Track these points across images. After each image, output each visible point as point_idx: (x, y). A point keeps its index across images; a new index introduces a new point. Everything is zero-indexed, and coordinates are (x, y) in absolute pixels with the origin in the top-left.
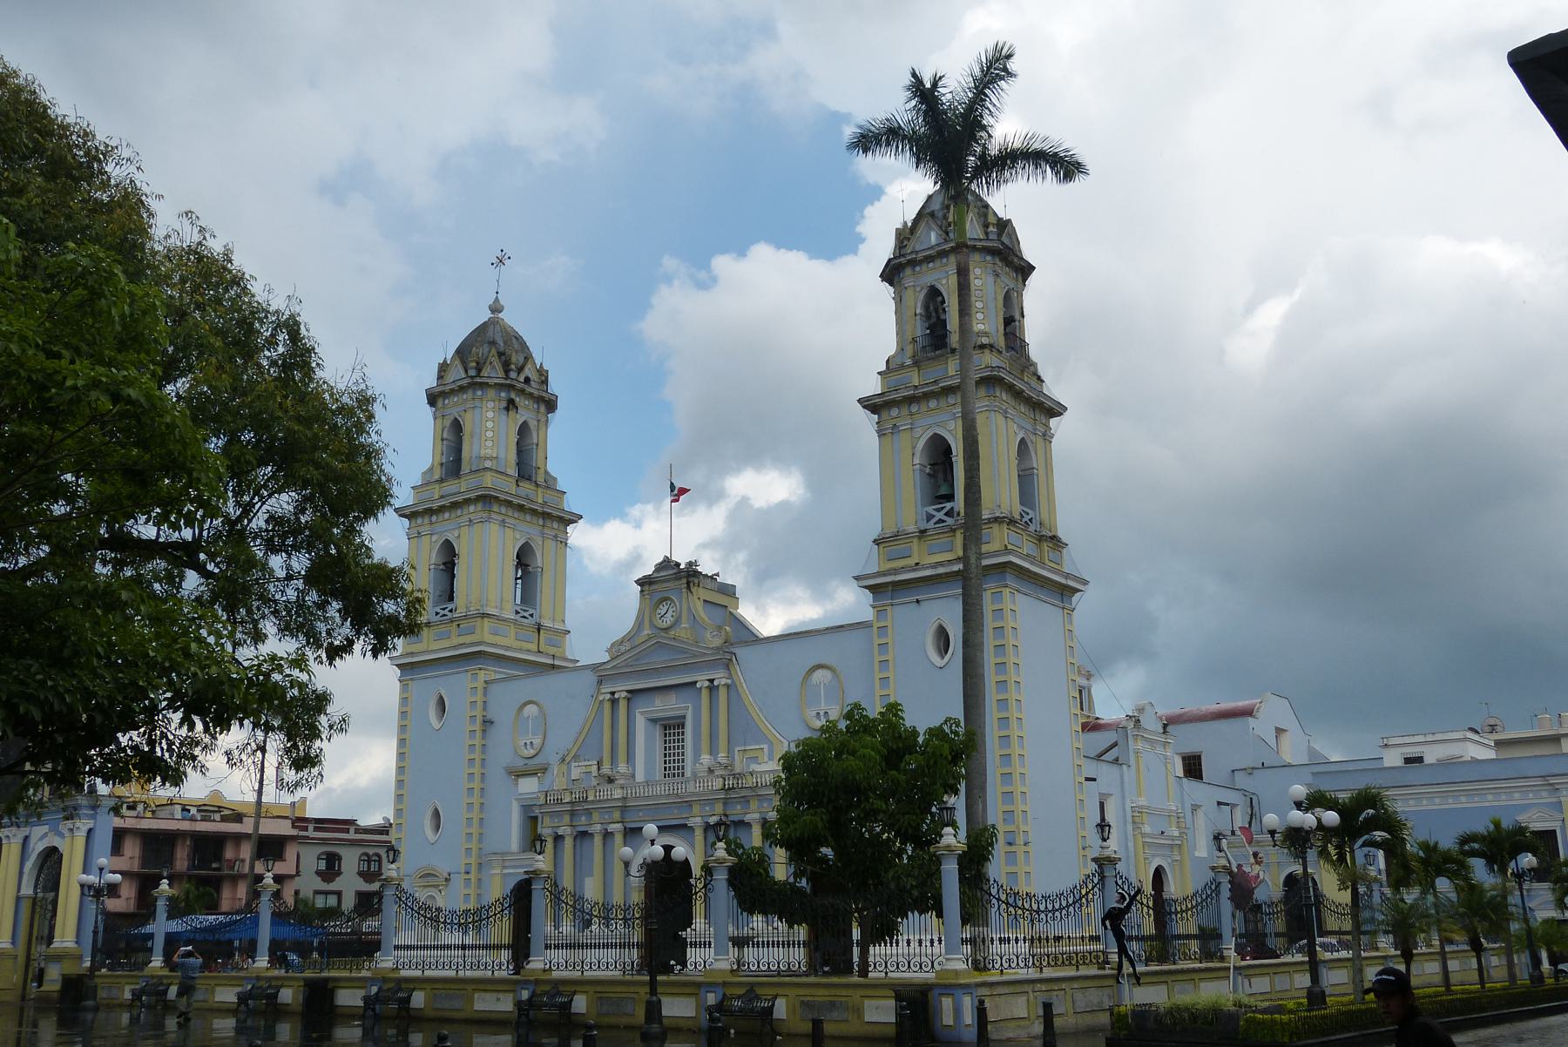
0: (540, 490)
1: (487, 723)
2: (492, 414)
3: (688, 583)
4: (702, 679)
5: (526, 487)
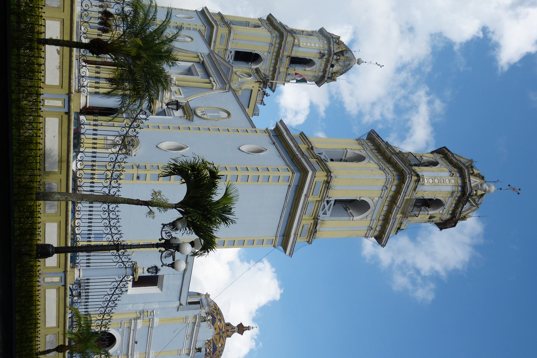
0: (285, 70)
2: (318, 46)
3: (260, 82)
5: (286, 61)
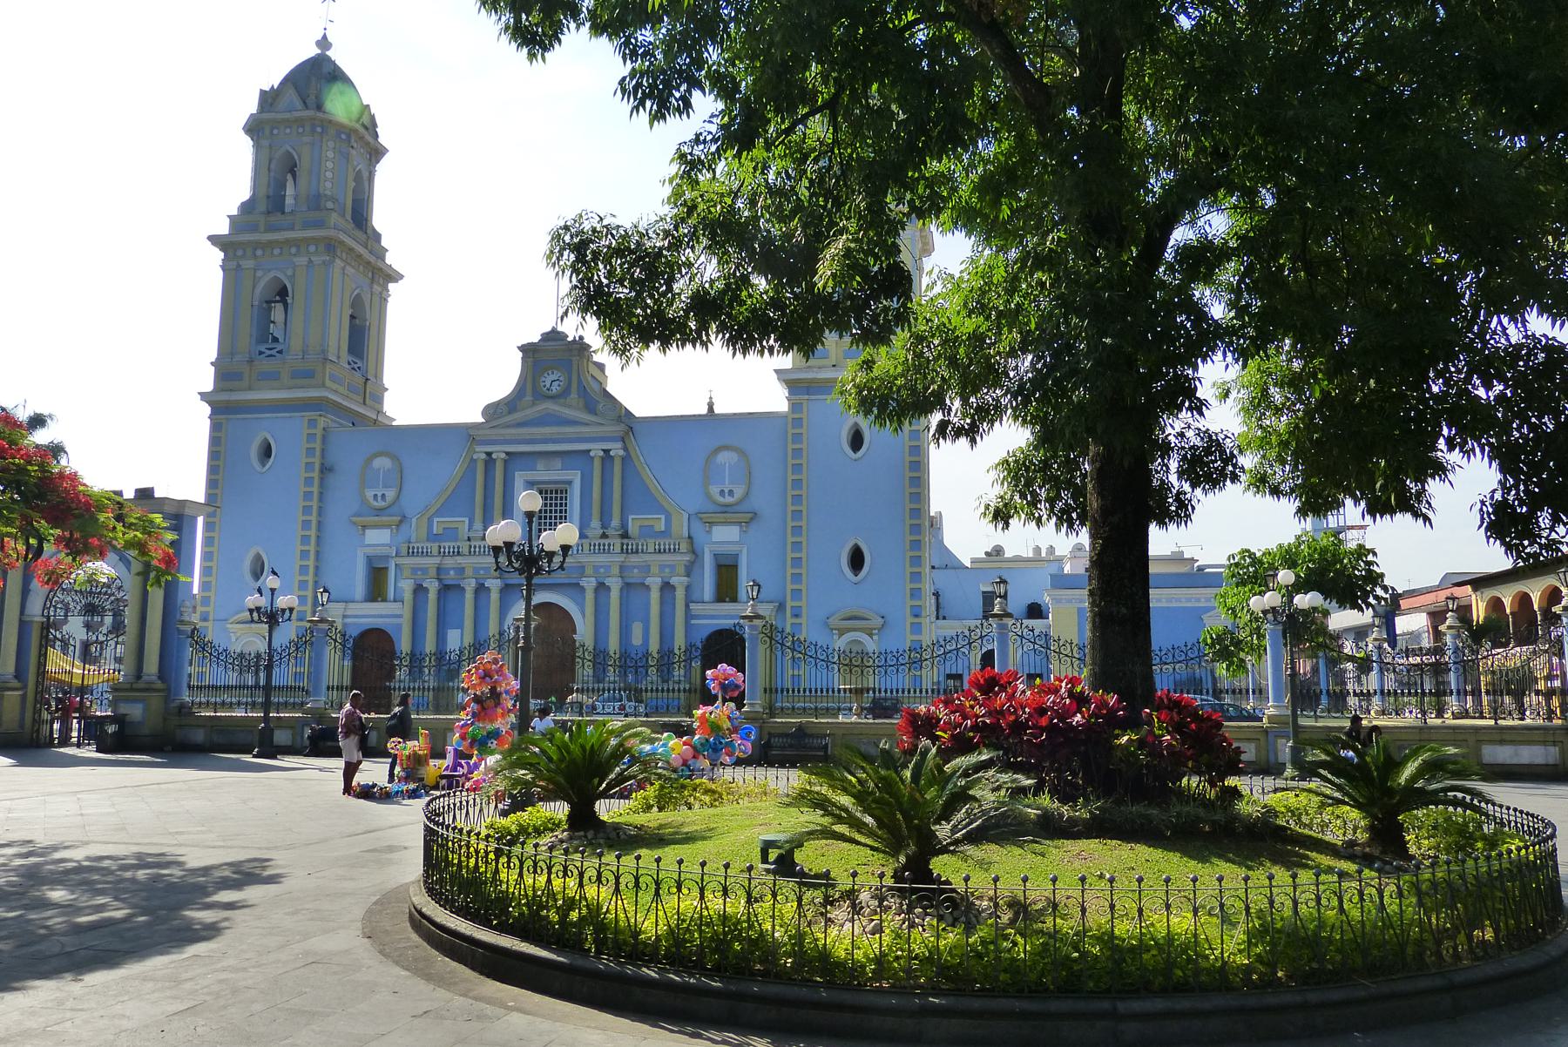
1: (326, 470)
4: (596, 449)
